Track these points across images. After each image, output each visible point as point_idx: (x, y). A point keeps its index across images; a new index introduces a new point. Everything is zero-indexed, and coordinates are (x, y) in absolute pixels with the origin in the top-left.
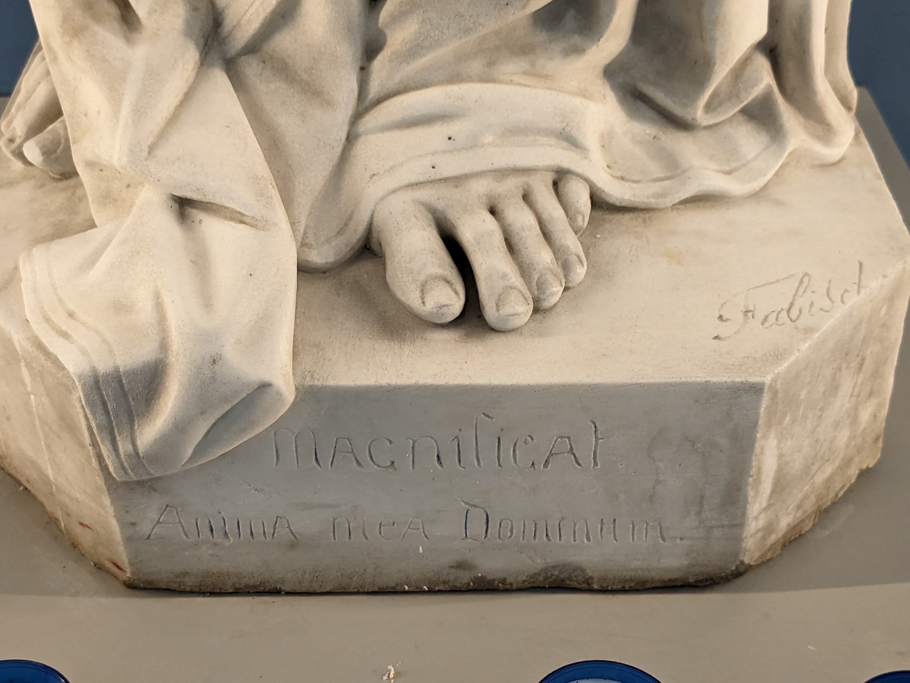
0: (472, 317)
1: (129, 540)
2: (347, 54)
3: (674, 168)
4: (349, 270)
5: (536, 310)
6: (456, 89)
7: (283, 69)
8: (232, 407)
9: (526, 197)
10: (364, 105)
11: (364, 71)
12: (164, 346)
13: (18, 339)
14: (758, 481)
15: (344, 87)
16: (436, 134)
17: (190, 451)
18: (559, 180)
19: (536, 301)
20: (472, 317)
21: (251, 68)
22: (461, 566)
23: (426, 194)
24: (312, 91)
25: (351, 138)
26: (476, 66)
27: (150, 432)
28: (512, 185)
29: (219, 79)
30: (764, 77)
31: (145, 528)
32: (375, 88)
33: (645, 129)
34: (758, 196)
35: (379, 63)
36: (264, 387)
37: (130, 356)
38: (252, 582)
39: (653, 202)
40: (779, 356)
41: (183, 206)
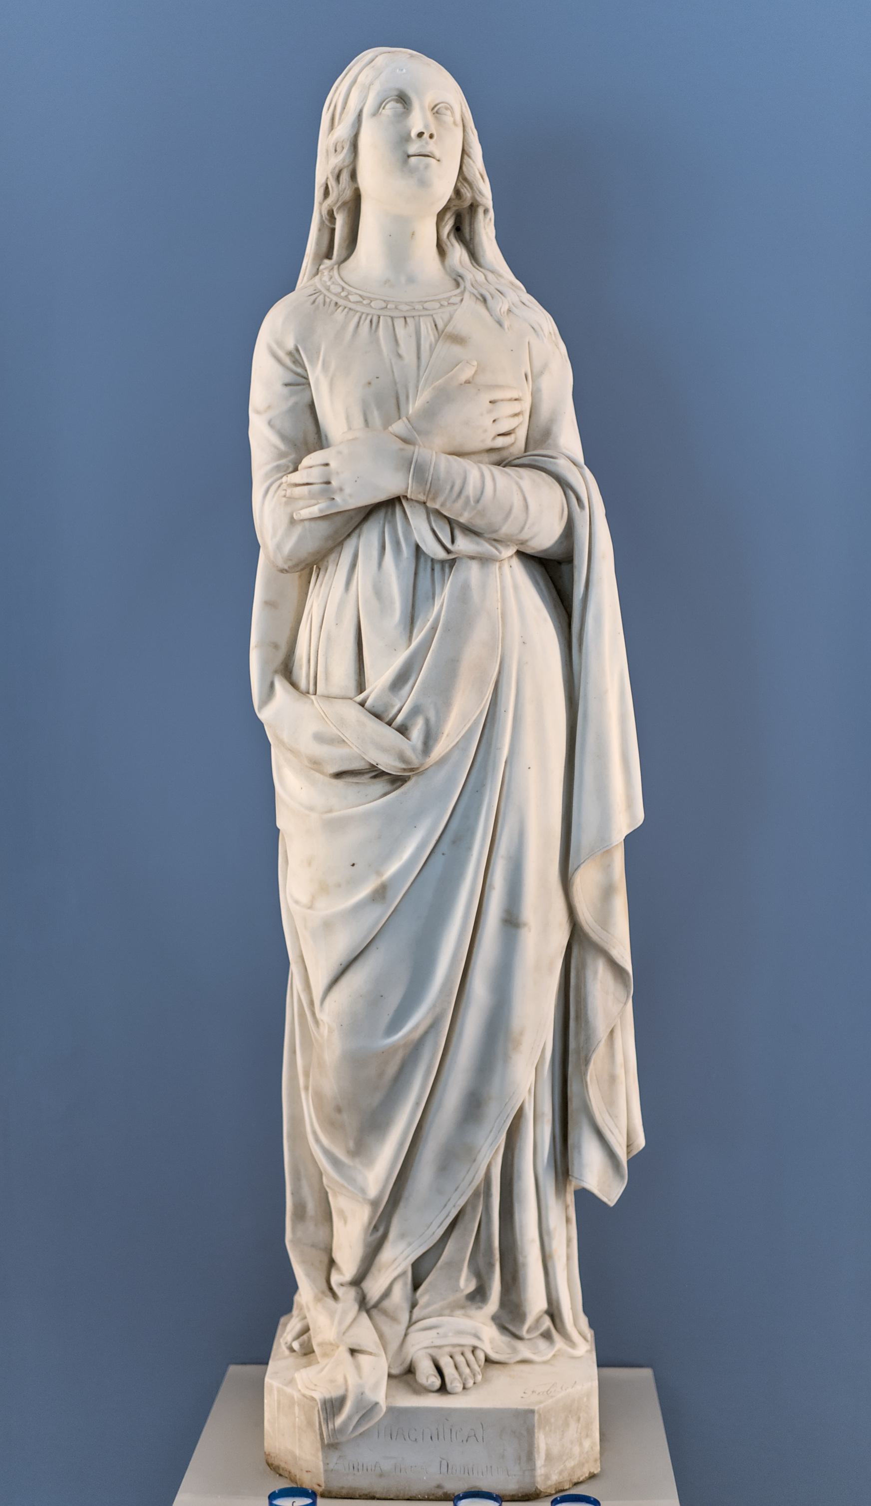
0: (443, 1389)
1: (326, 1471)
2: (406, 1306)
3: (514, 1350)
4: (406, 1375)
5: (464, 1388)
7: (385, 1313)
8: (367, 1410)
9: (462, 1354)
10: (411, 1323)
11: (411, 1312)
12: (347, 1390)
13: (296, 1395)
14: (539, 1453)
15: (404, 1317)
16: (433, 1333)
17: (351, 1428)
18: (474, 1350)
19: (464, 1384)
20: (443, 1389)
21: (374, 1312)
22: (439, 1487)
23: (430, 1351)
24: (394, 1319)
25: (406, 1335)
26: (447, 1312)
27: (339, 1420)
28: (458, 1350)
30: (547, 1323)
31: (331, 1466)
32: (414, 1317)
33: (506, 1339)
35: (416, 1310)
36: (377, 1404)
37: (335, 1393)
38: (366, 1492)
39: (507, 1361)
40: (541, 1402)
41: (353, 1352)
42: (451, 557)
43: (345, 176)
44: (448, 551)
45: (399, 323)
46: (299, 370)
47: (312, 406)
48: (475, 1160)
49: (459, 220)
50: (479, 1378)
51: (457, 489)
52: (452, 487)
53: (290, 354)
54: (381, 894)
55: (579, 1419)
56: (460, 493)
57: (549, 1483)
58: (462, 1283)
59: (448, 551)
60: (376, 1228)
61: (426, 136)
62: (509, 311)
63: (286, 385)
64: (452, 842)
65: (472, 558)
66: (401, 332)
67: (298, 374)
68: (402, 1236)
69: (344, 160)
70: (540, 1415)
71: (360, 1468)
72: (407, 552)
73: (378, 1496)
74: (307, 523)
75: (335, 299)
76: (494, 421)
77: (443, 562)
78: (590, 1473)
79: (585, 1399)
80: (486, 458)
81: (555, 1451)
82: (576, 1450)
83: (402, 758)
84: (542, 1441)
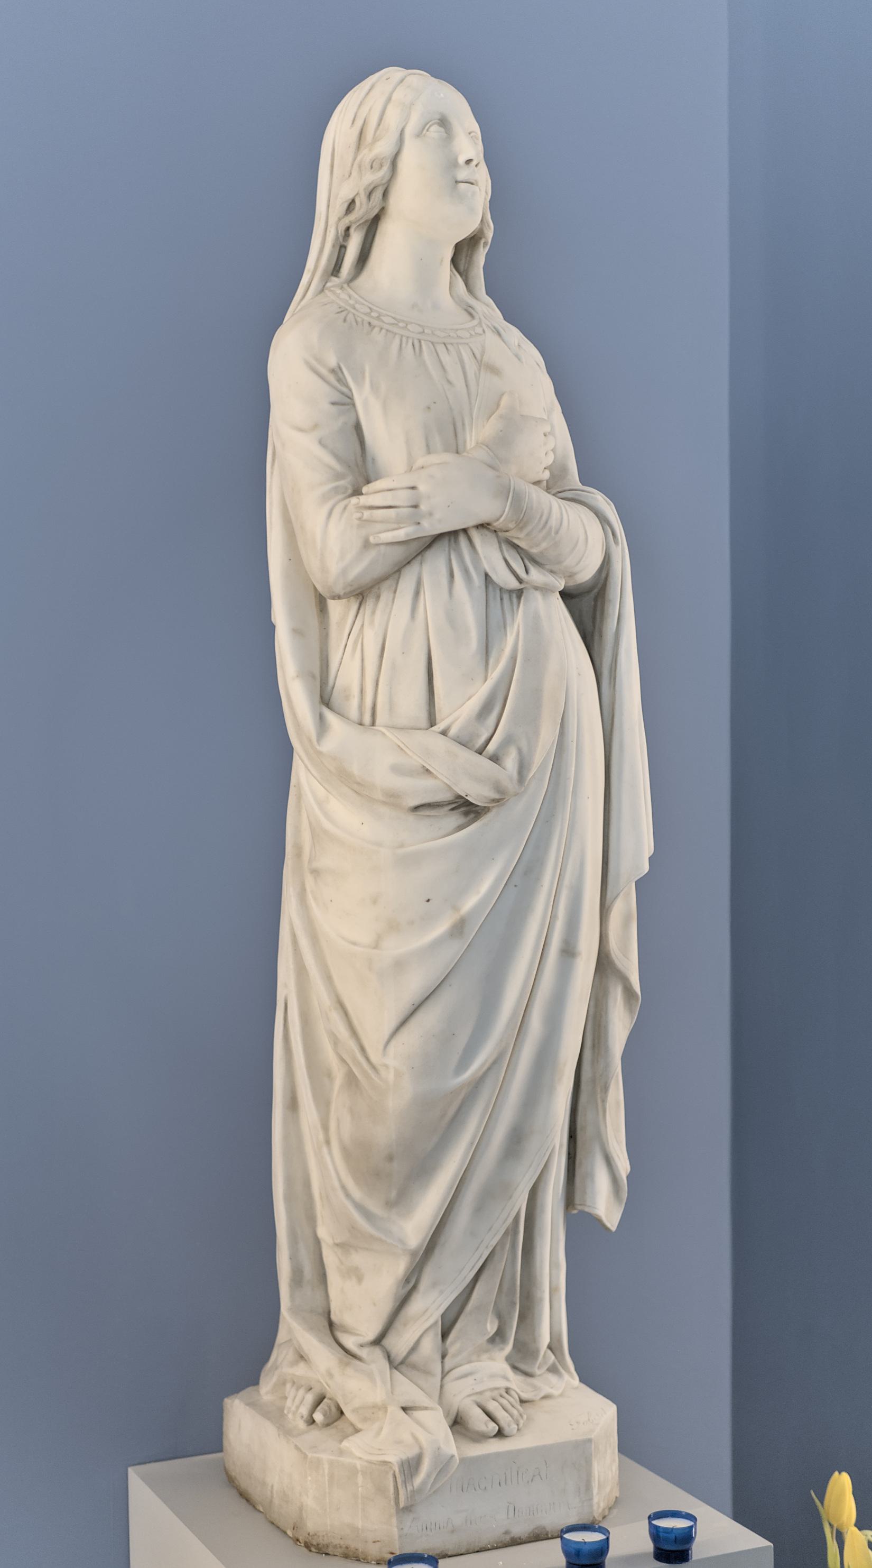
1: (400, 1536)
2: (438, 1357)
6: (473, 1364)
7: (414, 1367)
8: (443, 1465)
9: (501, 1396)
10: (444, 1375)
12: (421, 1448)
13: (359, 1464)
16: (470, 1380)
20: (500, 1434)
22: (507, 1533)
23: (474, 1398)
27: (418, 1481)
30: (552, 1358)
32: (447, 1368)
34: (561, 1395)
35: (447, 1359)
36: (453, 1456)
37: (411, 1453)
41: (404, 1409)
42: (522, 586)
43: (378, 194)
44: (520, 581)
45: (441, 349)
46: (344, 389)
47: (358, 427)
48: (510, 1198)
49: (462, 253)
51: (544, 518)
52: (541, 516)
53: (333, 371)
54: (459, 929)
56: (546, 523)
58: (489, 1326)
59: (520, 581)
60: (407, 1281)
61: (474, 163)
63: (333, 404)
64: (524, 876)
65: (536, 588)
66: (446, 358)
67: (343, 393)
68: (435, 1285)
69: (383, 177)
71: (433, 1526)
72: (478, 581)
73: (449, 1554)
74: (382, 548)
75: (367, 319)
77: (510, 592)
83: (498, 788)
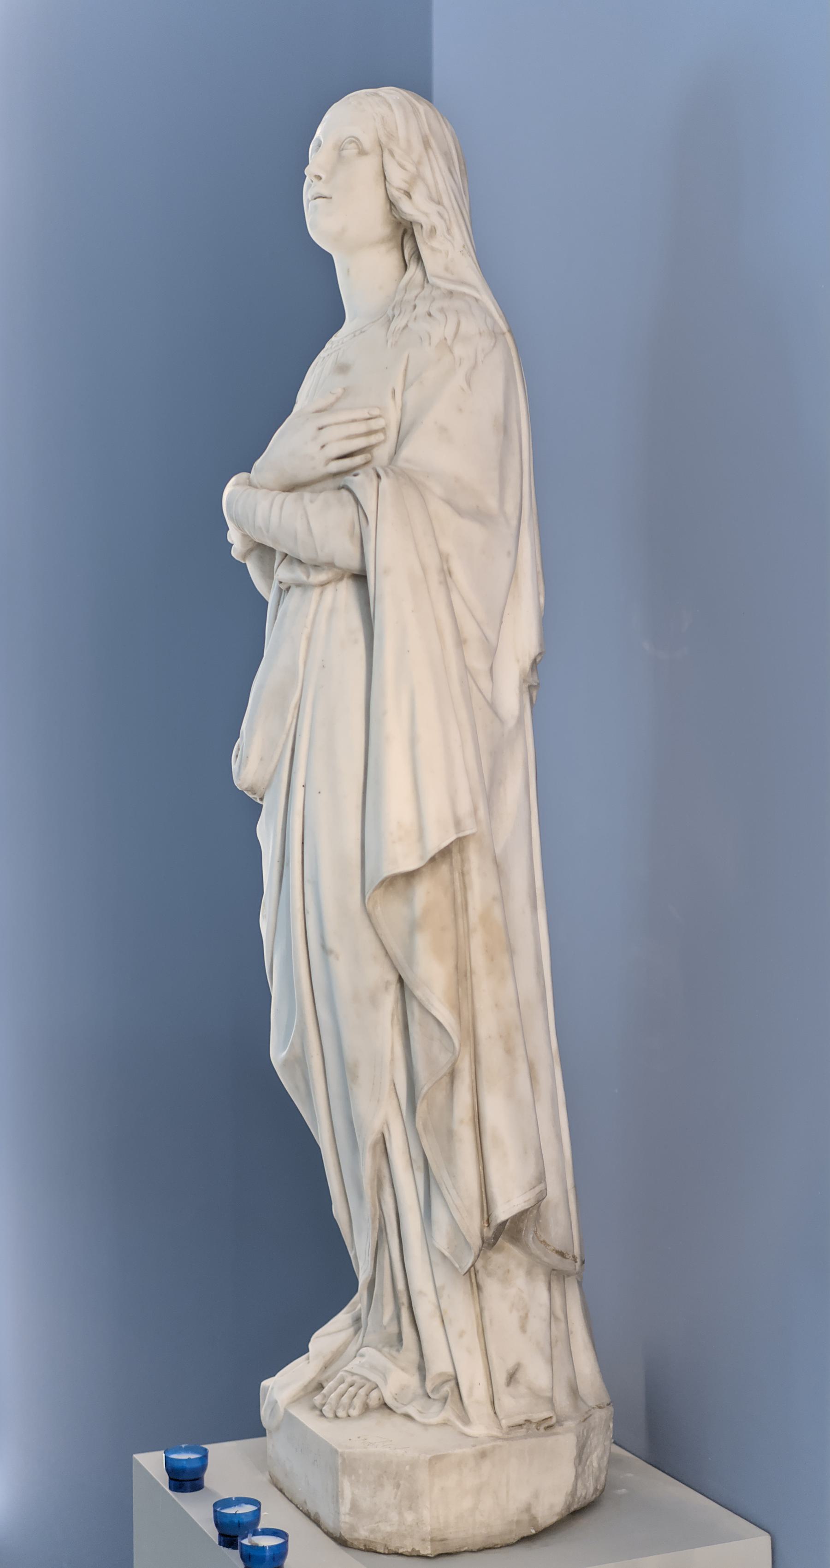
14: (343, 1498)
29: (351, 1330)
50: (354, 1412)
55: (398, 1486)
57: (356, 1535)
62: (406, 326)
70: (344, 1460)
76: (323, 447)
78: (413, 1550)
79: (407, 1468)
80: (332, 483)
81: (365, 1505)
82: (394, 1516)
84: (347, 1489)
